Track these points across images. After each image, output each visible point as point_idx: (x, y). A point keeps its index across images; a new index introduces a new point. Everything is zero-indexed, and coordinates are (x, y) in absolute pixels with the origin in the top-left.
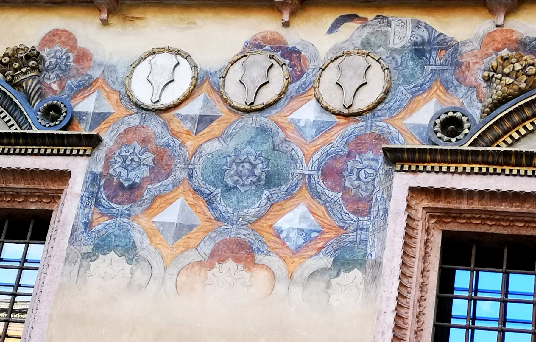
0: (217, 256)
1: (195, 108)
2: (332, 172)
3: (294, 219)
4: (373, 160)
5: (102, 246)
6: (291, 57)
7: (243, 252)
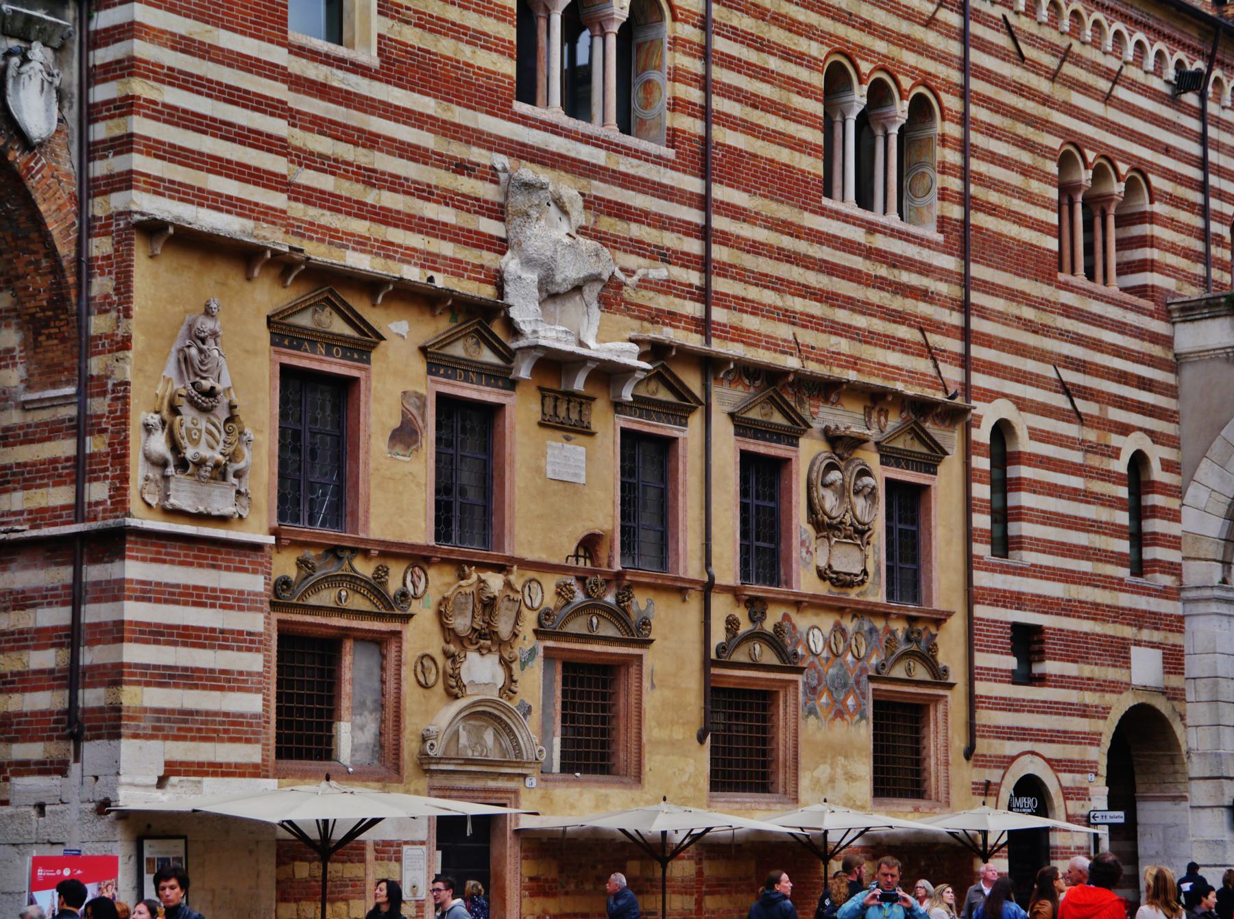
0: (836, 716)
1: (824, 655)
2: (858, 683)
4: (864, 678)
6: (843, 632)
7: (840, 714)
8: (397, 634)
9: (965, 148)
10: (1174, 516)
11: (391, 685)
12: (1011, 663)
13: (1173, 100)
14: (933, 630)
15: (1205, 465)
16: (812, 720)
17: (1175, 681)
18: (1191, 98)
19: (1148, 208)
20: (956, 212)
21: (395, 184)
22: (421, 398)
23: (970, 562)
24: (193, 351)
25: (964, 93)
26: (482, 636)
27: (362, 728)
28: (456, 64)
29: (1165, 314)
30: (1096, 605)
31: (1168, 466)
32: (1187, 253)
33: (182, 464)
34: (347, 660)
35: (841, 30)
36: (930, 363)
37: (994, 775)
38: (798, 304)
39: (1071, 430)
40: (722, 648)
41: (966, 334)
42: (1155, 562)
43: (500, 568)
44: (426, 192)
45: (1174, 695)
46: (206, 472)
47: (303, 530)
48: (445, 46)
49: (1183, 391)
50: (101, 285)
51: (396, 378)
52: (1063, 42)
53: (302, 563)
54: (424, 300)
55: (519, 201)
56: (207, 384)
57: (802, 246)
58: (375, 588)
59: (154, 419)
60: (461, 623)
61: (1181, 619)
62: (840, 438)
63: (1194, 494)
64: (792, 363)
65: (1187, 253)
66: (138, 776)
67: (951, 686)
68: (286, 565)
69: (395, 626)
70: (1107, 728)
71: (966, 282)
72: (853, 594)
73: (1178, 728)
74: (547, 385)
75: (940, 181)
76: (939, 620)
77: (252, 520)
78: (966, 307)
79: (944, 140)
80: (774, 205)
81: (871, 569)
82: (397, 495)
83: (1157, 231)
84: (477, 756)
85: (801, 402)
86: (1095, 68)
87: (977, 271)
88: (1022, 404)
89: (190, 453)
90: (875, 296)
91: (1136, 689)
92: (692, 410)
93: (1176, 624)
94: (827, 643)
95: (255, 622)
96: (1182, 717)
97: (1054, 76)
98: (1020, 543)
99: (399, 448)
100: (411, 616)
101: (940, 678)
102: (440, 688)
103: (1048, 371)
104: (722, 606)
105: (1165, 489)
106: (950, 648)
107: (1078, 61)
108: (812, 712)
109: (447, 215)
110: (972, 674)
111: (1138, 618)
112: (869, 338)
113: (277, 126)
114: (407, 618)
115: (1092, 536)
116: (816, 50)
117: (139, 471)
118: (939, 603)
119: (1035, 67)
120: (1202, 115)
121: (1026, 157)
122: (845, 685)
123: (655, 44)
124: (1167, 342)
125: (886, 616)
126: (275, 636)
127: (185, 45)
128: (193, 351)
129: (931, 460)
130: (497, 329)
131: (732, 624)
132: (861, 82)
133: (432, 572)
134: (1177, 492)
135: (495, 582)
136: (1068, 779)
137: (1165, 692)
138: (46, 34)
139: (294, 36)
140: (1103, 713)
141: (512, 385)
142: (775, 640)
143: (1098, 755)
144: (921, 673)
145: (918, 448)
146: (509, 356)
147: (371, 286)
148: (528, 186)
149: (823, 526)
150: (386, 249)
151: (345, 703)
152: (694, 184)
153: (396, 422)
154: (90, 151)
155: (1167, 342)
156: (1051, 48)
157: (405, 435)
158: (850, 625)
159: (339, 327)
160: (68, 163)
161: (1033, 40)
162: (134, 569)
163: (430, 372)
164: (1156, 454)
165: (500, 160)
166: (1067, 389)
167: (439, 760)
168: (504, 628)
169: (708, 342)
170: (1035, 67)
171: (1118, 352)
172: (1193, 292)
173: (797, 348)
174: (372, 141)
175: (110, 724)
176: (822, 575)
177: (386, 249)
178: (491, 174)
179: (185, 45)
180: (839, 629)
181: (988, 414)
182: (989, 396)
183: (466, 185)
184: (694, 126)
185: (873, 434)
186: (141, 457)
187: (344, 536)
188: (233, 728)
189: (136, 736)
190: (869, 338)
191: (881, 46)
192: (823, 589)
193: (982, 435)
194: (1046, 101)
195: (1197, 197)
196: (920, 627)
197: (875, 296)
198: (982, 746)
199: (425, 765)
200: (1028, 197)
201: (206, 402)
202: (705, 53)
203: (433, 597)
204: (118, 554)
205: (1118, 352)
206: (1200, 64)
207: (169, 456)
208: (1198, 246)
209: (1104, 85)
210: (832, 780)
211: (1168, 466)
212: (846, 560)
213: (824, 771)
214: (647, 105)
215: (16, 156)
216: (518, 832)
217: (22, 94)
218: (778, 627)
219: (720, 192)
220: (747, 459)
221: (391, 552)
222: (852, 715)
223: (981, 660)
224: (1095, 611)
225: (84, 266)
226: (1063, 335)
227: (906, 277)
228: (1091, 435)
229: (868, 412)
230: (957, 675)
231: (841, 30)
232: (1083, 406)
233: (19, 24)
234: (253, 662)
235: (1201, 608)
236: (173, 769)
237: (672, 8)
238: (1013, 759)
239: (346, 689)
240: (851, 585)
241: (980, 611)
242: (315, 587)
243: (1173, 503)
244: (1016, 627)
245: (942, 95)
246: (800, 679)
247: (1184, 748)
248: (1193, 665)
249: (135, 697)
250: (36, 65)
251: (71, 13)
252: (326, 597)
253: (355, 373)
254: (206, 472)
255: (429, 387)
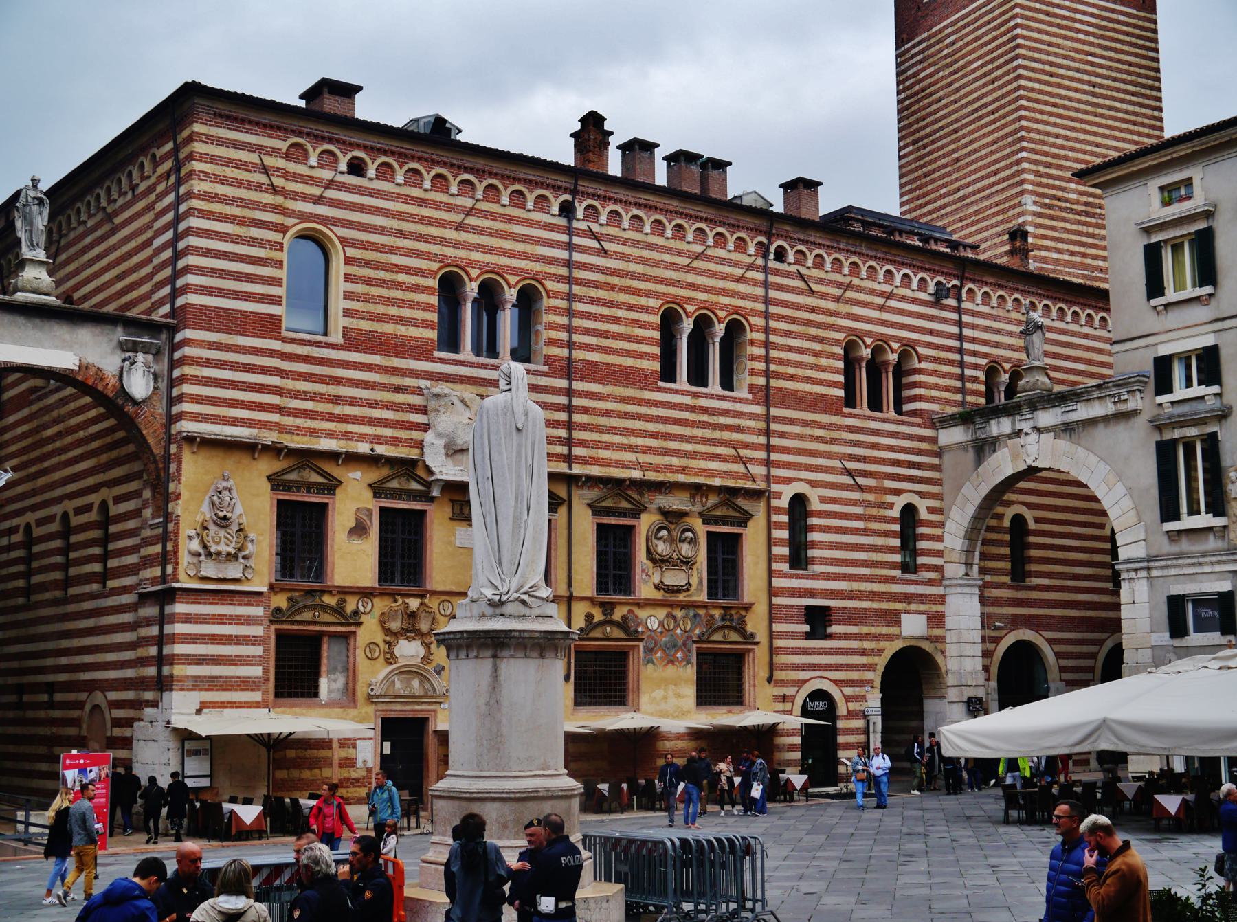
2: (684, 645)
3: (679, 655)
4: (690, 642)
5: (649, 662)
6: (674, 617)
7: (672, 662)
8: (354, 633)
9: (767, 345)
10: (940, 539)
11: (351, 658)
12: (806, 628)
13: (937, 303)
14: (743, 613)
15: (954, 509)
16: (650, 666)
17: (937, 632)
18: (951, 302)
19: (917, 365)
20: (761, 381)
21: (353, 402)
22: (370, 512)
23: (771, 574)
24: (215, 498)
25: (766, 315)
26: (410, 632)
27: (335, 681)
28: (395, 337)
29: (932, 426)
30: (874, 593)
31: (931, 510)
32: (948, 389)
33: (209, 555)
34: (325, 647)
35: (672, 290)
36: (742, 466)
37: (790, 691)
38: (640, 441)
39: (855, 495)
40: (581, 630)
41: (769, 448)
42: (923, 565)
43: (422, 596)
44: (374, 404)
45: (940, 640)
46: (223, 557)
47: (288, 583)
48: (388, 328)
49: (944, 467)
50: (173, 467)
51: (353, 500)
52: (847, 280)
53: (289, 599)
54: (372, 460)
55: (433, 404)
56: (221, 514)
57: (643, 410)
58: (339, 610)
59: (193, 533)
60: (395, 625)
61: (943, 597)
62: (669, 512)
63: (949, 525)
64: (636, 474)
65: (948, 389)
66: (182, 709)
67: (757, 643)
68: (280, 601)
69: (352, 629)
70: (881, 662)
71: (767, 418)
72: (681, 597)
73: (939, 659)
74: (456, 498)
75: (750, 365)
76: (748, 607)
77: (256, 580)
78: (768, 433)
79: (752, 343)
80: (622, 389)
81: (694, 581)
82: (353, 560)
83: (923, 378)
84: (407, 693)
85: (641, 494)
86: (872, 292)
87: (774, 411)
88: (813, 484)
89: (212, 550)
90: (698, 432)
91: (904, 638)
92: (560, 504)
93: (941, 599)
94: (661, 624)
95: (258, 631)
96: (943, 652)
97: (838, 300)
98: (812, 561)
99: (354, 537)
100: (361, 624)
101: (749, 639)
102: (382, 659)
103: (837, 464)
104: (580, 610)
105: (930, 524)
106: (756, 623)
107: (858, 289)
108: (650, 661)
109: (388, 415)
110: (772, 636)
111: (908, 598)
112: (694, 455)
113: (275, 381)
114: (359, 624)
115: (870, 554)
116: (652, 303)
117: (184, 559)
118: (747, 598)
119: (823, 296)
120: (958, 310)
121: (817, 346)
122: (675, 646)
123: (539, 310)
124: (934, 440)
125: (705, 607)
126: (273, 637)
127: (217, 346)
128: (215, 498)
129: (744, 519)
130: (421, 473)
131: (589, 617)
132: (688, 316)
133: (376, 600)
134: (941, 525)
135: (414, 604)
136: (848, 691)
137: (928, 638)
138: (146, 349)
139: (284, 333)
140: (879, 652)
141: (432, 499)
142: (623, 625)
143: (876, 677)
144: (734, 637)
145: (732, 513)
146: (429, 485)
147: (333, 456)
148: (437, 396)
149: (658, 561)
150: (347, 436)
151: (323, 669)
152: (563, 383)
153: (353, 524)
154: (171, 402)
155: (934, 440)
156: (838, 284)
157: (359, 530)
158: (679, 614)
159: (315, 478)
160: (160, 408)
161: (820, 281)
162: (180, 608)
163: (375, 496)
164: (922, 505)
165: (423, 383)
166: (849, 473)
167: (378, 697)
168: (424, 626)
169: (570, 468)
170: (823, 296)
171: (892, 449)
172: (950, 410)
173: (639, 465)
174: (338, 381)
175: (163, 684)
176: (657, 587)
177: (347, 436)
178: (419, 391)
179: (217, 346)
180: (671, 616)
181: (788, 492)
182: (787, 481)
183: (401, 398)
184: (564, 352)
185: (694, 509)
186: (186, 552)
187: (316, 586)
188: (245, 684)
189: (182, 690)
190: (694, 455)
191: (703, 296)
192: (658, 595)
193: (784, 503)
194: (832, 313)
195: (957, 357)
196: (733, 612)
197: (698, 432)
198: (779, 675)
199: (370, 699)
200: (820, 368)
201: (224, 523)
202: (570, 313)
203: (377, 613)
204: (172, 601)
205: (892, 449)
206: (956, 282)
207: (201, 551)
208: (958, 384)
209: (880, 301)
210: (665, 698)
211: (931, 510)
212: (674, 578)
213: (659, 693)
214: (537, 343)
215: (130, 408)
216: (435, 732)
217: (132, 378)
218: (624, 618)
219: (577, 385)
220: (602, 530)
221: (345, 591)
222: (680, 662)
223: (777, 627)
224: (873, 596)
225: (167, 458)
226: (847, 443)
227: (722, 420)
228: (870, 497)
229: (693, 497)
230: (762, 636)
231: (672, 290)
232: (861, 481)
233: (130, 345)
234: (257, 651)
235: (953, 590)
236: (204, 706)
237: (547, 292)
238: (806, 681)
239: (324, 661)
240: (679, 591)
241: (776, 600)
242: (299, 611)
243: (937, 531)
244: (808, 608)
245: (750, 318)
246: (641, 644)
247: (943, 669)
248: (950, 623)
249: (179, 670)
250: (139, 364)
251: (164, 336)
252: (307, 616)
253: (326, 501)
254: (223, 557)
255: (374, 505)
